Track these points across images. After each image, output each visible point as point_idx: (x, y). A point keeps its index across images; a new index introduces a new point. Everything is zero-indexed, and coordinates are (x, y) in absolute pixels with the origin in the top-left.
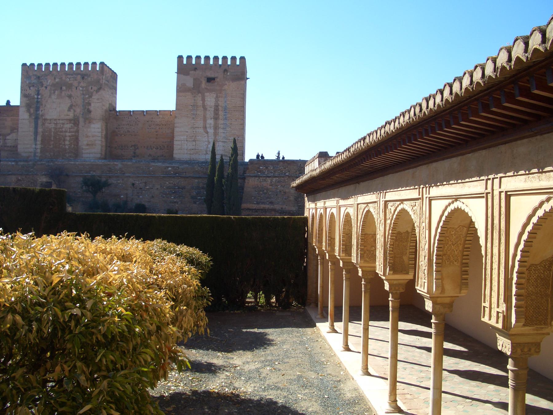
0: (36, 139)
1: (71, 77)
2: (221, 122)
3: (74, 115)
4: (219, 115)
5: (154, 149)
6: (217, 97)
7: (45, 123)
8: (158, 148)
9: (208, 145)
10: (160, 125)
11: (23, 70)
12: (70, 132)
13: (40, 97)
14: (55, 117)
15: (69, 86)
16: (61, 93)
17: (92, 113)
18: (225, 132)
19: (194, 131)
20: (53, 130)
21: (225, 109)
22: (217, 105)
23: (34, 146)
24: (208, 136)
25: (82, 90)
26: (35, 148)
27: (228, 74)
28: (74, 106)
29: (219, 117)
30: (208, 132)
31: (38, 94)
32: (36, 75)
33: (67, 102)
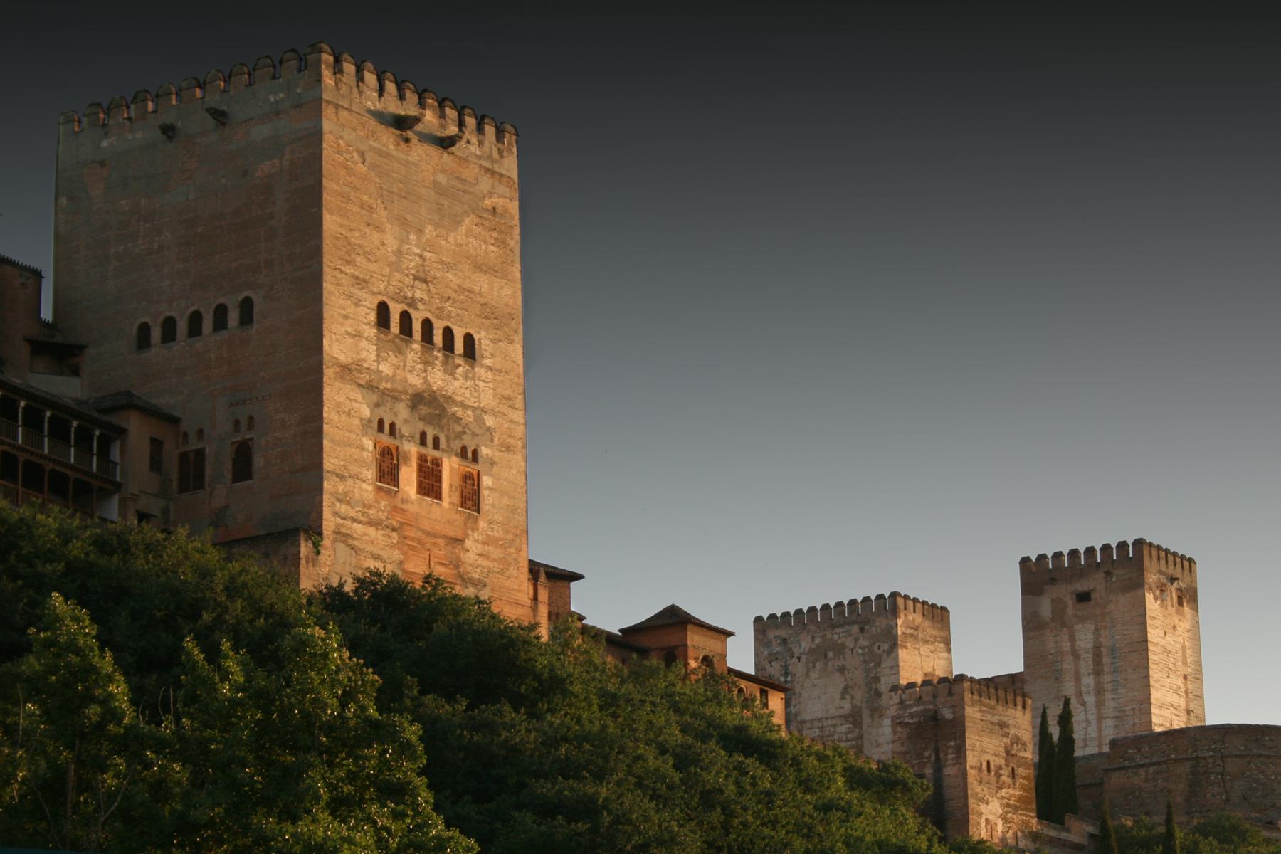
1: (841, 630)
2: (1107, 678)
3: (852, 706)
6: (1097, 629)
9: (1086, 728)
11: (756, 631)
12: (847, 741)
13: (789, 678)
14: (819, 715)
16: (826, 665)
18: (1117, 696)
21: (1113, 650)
24: (1086, 711)
25: (863, 654)
27: (1114, 579)
28: (852, 687)
30: (1085, 703)
31: (786, 674)
32: (779, 637)
33: (838, 682)
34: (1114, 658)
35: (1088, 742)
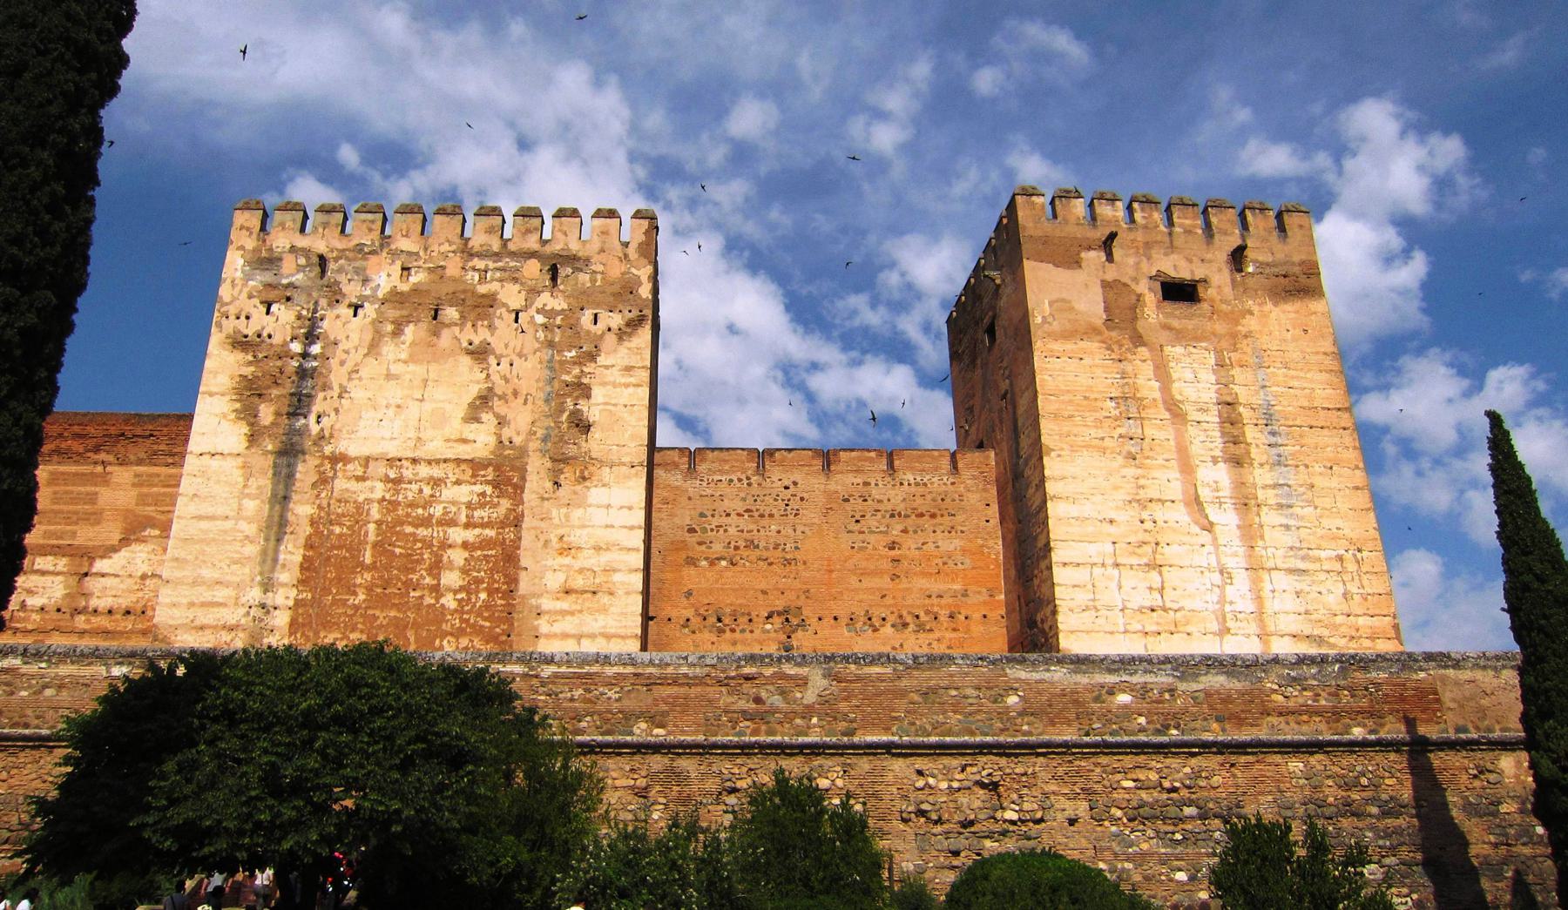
0: (275, 560)
1: (491, 265)
2: (1261, 476)
4: (1249, 444)
5: (888, 630)
6: (1220, 364)
7: (333, 478)
8: (905, 625)
9: (1221, 588)
10: (907, 516)
12: (467, 526)
14: (393, 450)
15: (481, 307)
16: (436, 334)
17: (595, 433)
19: (1145, 515)
20: (375, 513)
22: (1229, 399)
23: (255, 594)
26: (263, 606)
27: (1250, 269)
28: (503, 397)
29: (1248, 453)
30: (1212, 524)
31: (311, 337)
33: (467, 379)
34: (1273, 434)
35: (1230, 624)
